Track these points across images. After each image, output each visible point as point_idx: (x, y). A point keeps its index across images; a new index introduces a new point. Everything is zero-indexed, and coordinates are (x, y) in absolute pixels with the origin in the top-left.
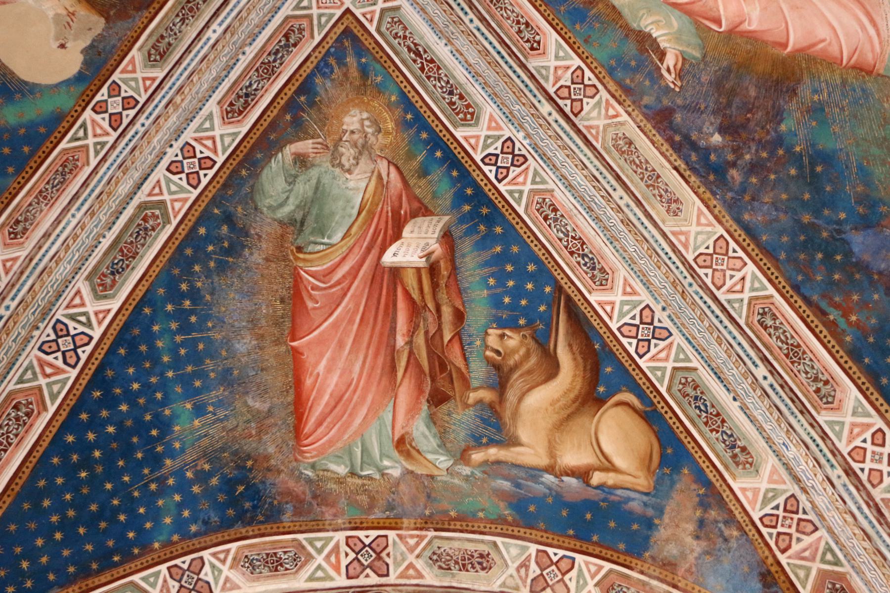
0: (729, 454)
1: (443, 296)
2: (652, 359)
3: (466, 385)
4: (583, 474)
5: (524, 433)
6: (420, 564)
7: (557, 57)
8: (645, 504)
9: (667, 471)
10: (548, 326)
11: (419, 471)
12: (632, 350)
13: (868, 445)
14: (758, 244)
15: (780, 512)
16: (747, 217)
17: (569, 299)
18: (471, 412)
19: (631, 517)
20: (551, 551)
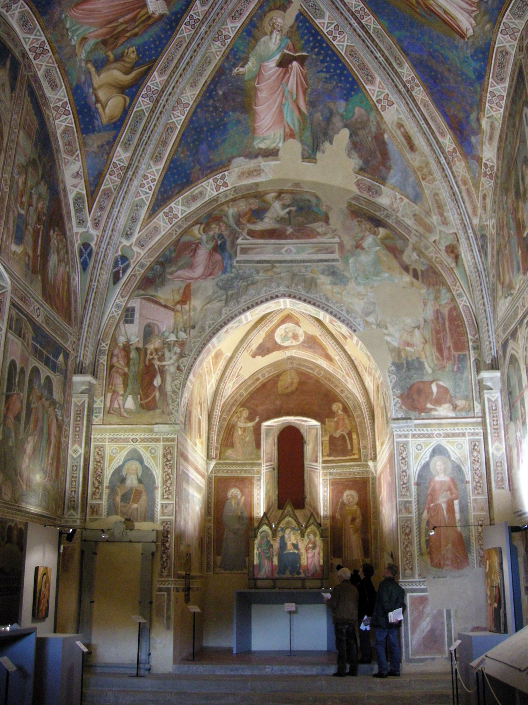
0: (126, 141)
1: (141, 27)
2: (143, 101)
3: (112, 50)
4: (98, 101)
5: (103, 76)
6: (43, 68)
7: (232, 28)
8: (99, 126)
9: (112, 126)
10: (142, 64)
11: (77, 50)
12: (143, 93)
13: (150, 179)
14: (192, 116)
15: (119, 166)
16: (199, 110)
17: (152, 66)
18: (104, 55)
19: (91, 122)
20: (69, 105)
